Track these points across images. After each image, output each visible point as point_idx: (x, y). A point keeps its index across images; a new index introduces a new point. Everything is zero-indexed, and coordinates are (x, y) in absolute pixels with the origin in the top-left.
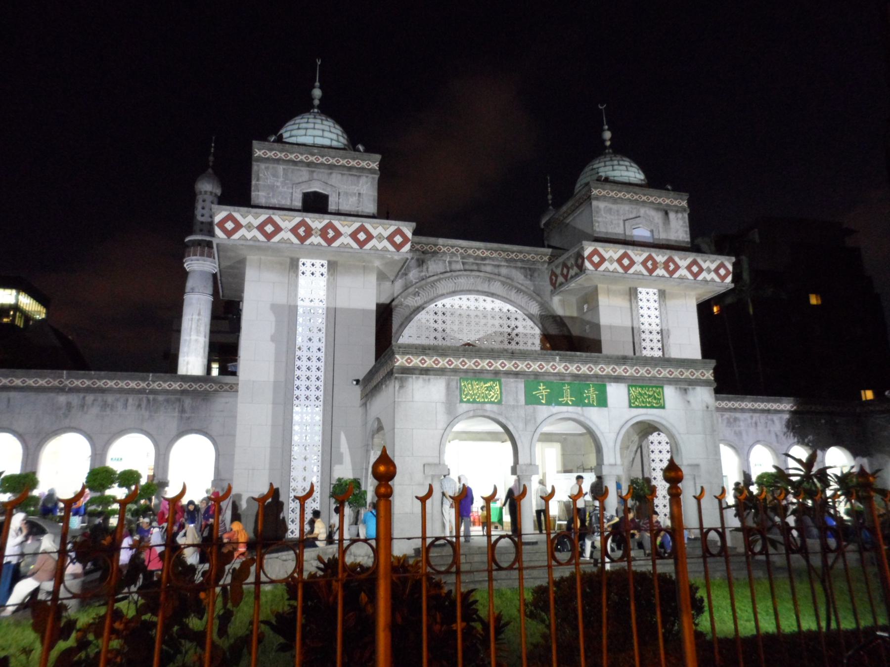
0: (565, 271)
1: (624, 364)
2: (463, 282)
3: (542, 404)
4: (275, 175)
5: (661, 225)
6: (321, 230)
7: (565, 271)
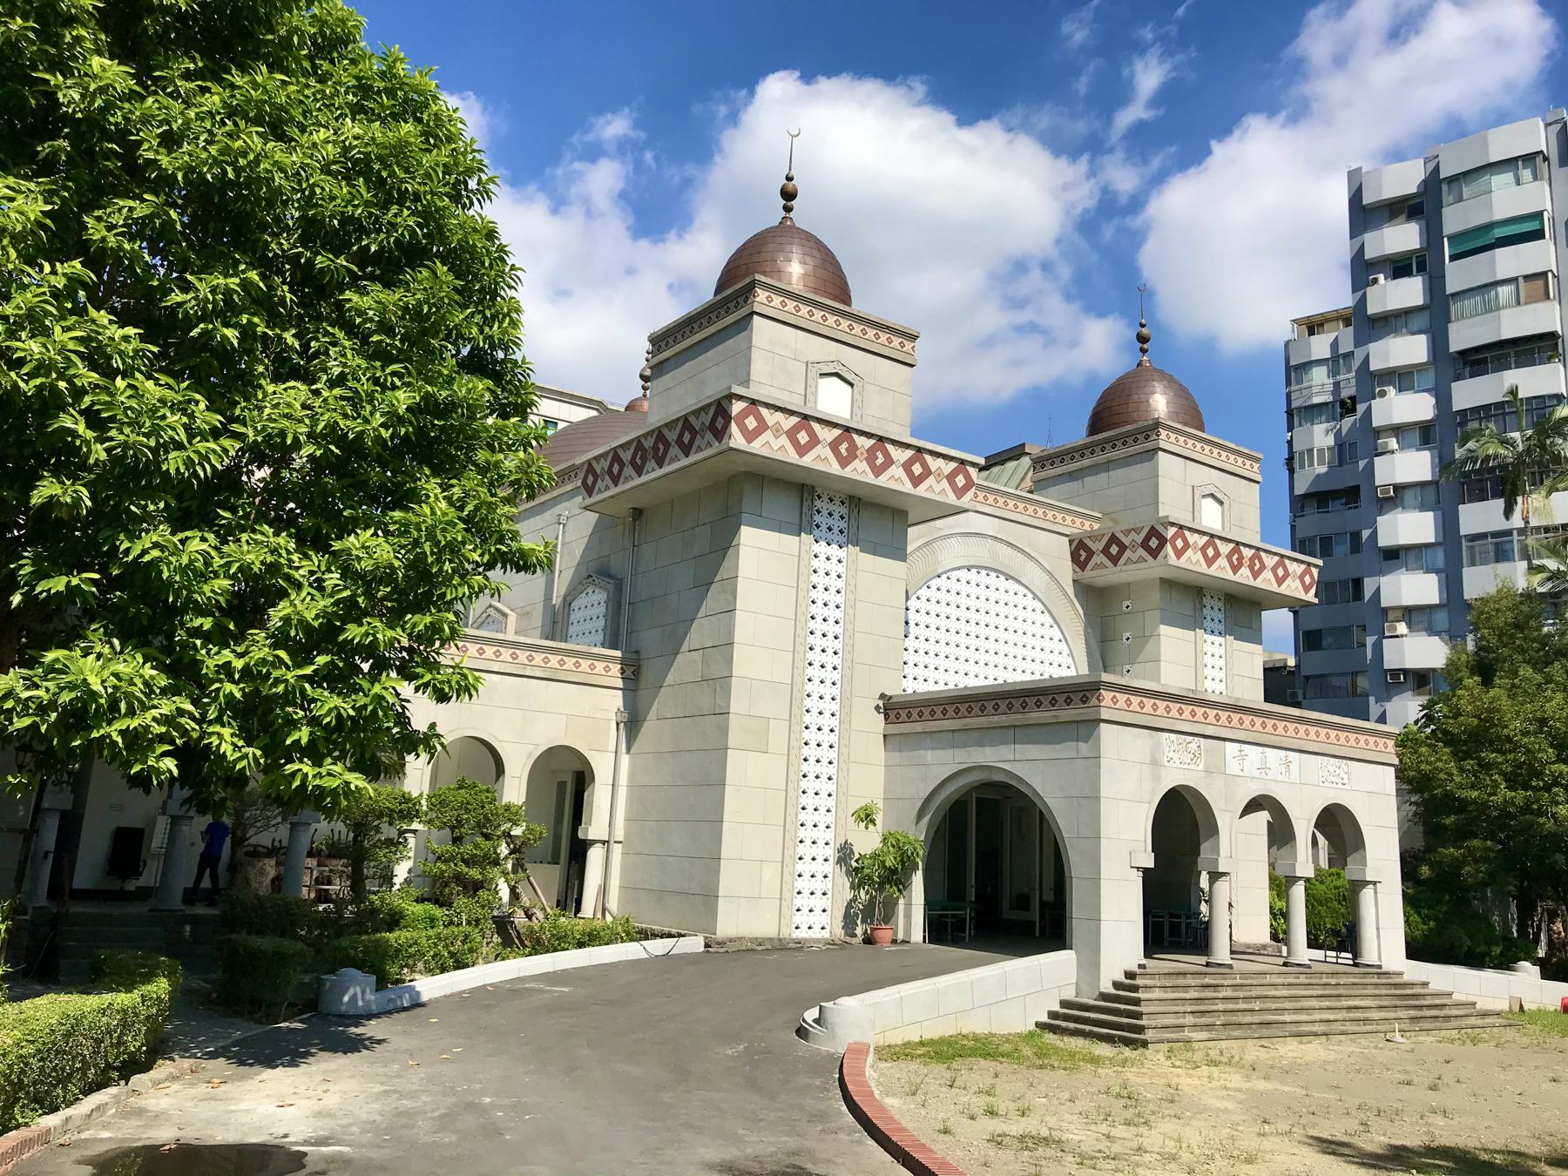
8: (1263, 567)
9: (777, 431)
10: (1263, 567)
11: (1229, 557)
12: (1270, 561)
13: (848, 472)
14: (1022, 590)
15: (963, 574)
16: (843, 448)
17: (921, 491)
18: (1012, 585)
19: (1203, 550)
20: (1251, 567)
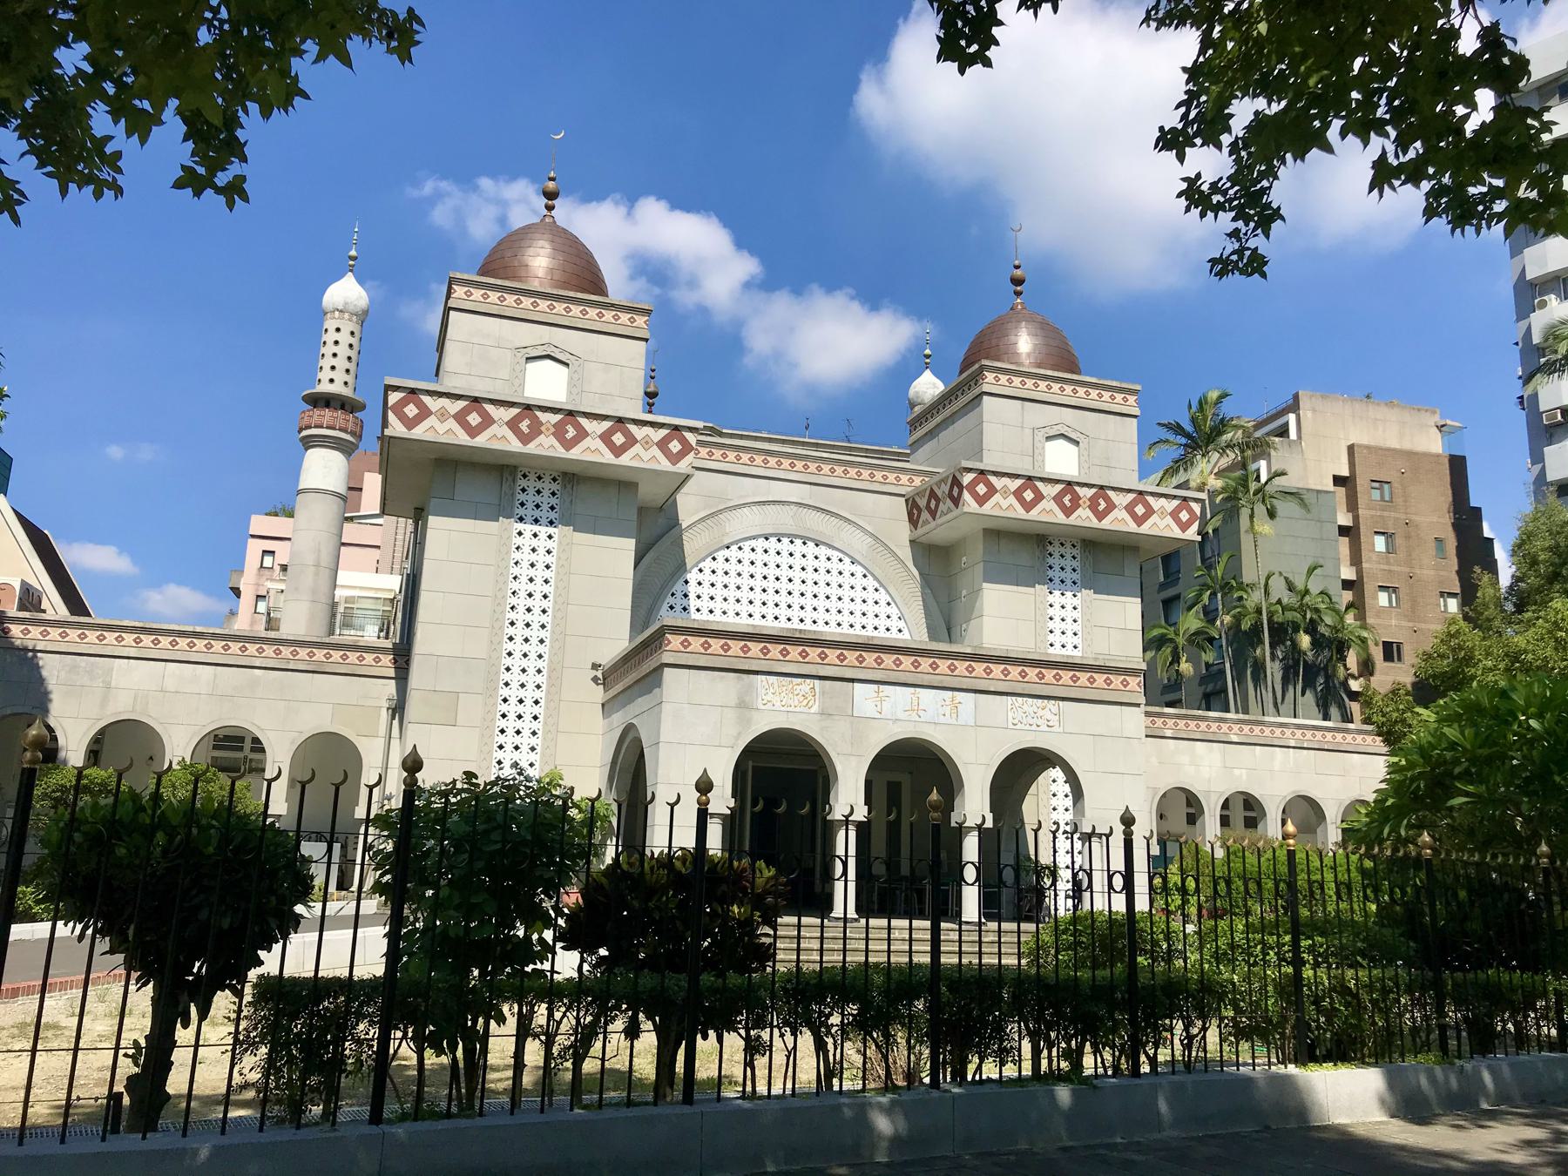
9: (647, 443)
13: (1073, 520)
14: (835, 555)
15: (760, 544)
18: (823, 551)
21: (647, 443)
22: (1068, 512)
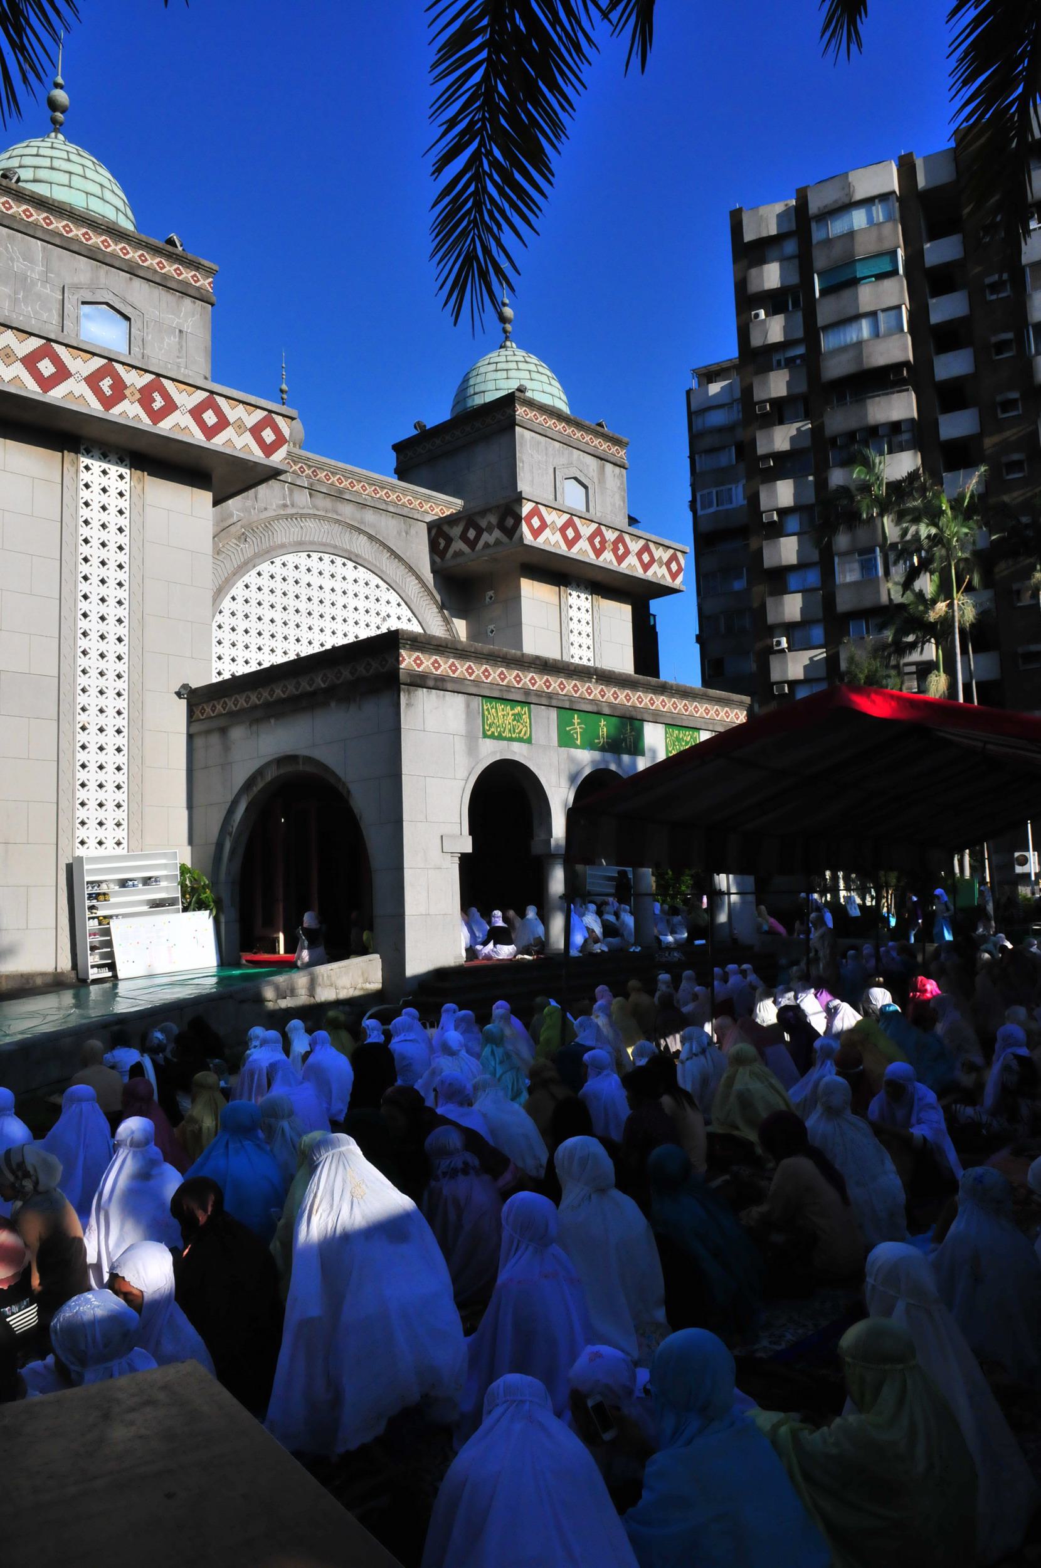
0: (472, 534)
1: (662, 694)
2: (314, 530)
3: (577, 747)
4: (28, 257)
5: (596, 480)
6: (140, 391)
7: (472, 534)
8: (627, 552)
10: (627, 552)
11: (591, 539)
12: (635, 546)
16: (106, 384)
17: (218, 442)
19: (563, 530)
20: (615, 550)
21: (240, 426)
22: (598, 553)
